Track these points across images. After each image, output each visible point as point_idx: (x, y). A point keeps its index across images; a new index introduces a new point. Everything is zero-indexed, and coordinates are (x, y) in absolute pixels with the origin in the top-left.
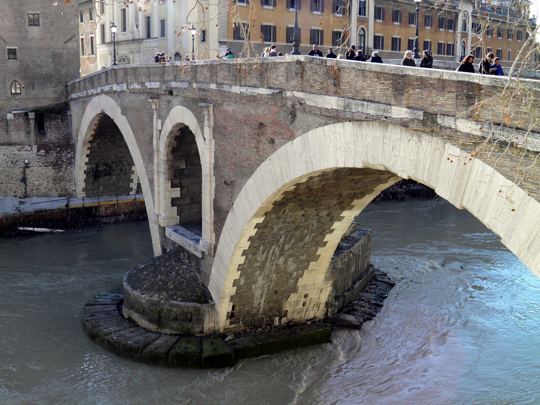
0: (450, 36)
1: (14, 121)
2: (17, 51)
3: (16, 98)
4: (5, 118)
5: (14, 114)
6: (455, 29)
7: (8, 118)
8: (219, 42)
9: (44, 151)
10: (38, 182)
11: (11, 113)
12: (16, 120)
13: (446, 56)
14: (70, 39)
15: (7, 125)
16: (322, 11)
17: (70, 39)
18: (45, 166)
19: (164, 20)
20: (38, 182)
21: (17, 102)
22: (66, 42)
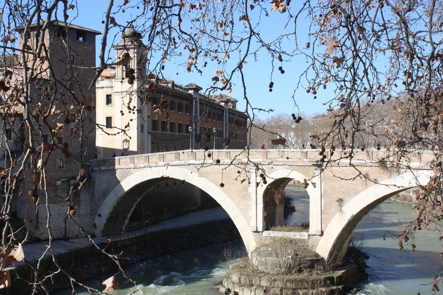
0: (221, 125)
1: (61, 186)
2: (63, 138)
3: (61, 170)
4: (55, 184)
5: (62, 181)
6: (222, 121)
7: (57, 184)
8: (148, 132)
9: (77, 206)
10: (73, 228)
11: (60, 180)
12: (62, 185)
13: (219, 138)
14: (91, 131)
15: (57, 189)
16: (174, 110)
17: (91, 131)
18: (78, 216)
19: (111, 118)
20: (73, 228)
21: (61, 173)
22: (89, 133)
